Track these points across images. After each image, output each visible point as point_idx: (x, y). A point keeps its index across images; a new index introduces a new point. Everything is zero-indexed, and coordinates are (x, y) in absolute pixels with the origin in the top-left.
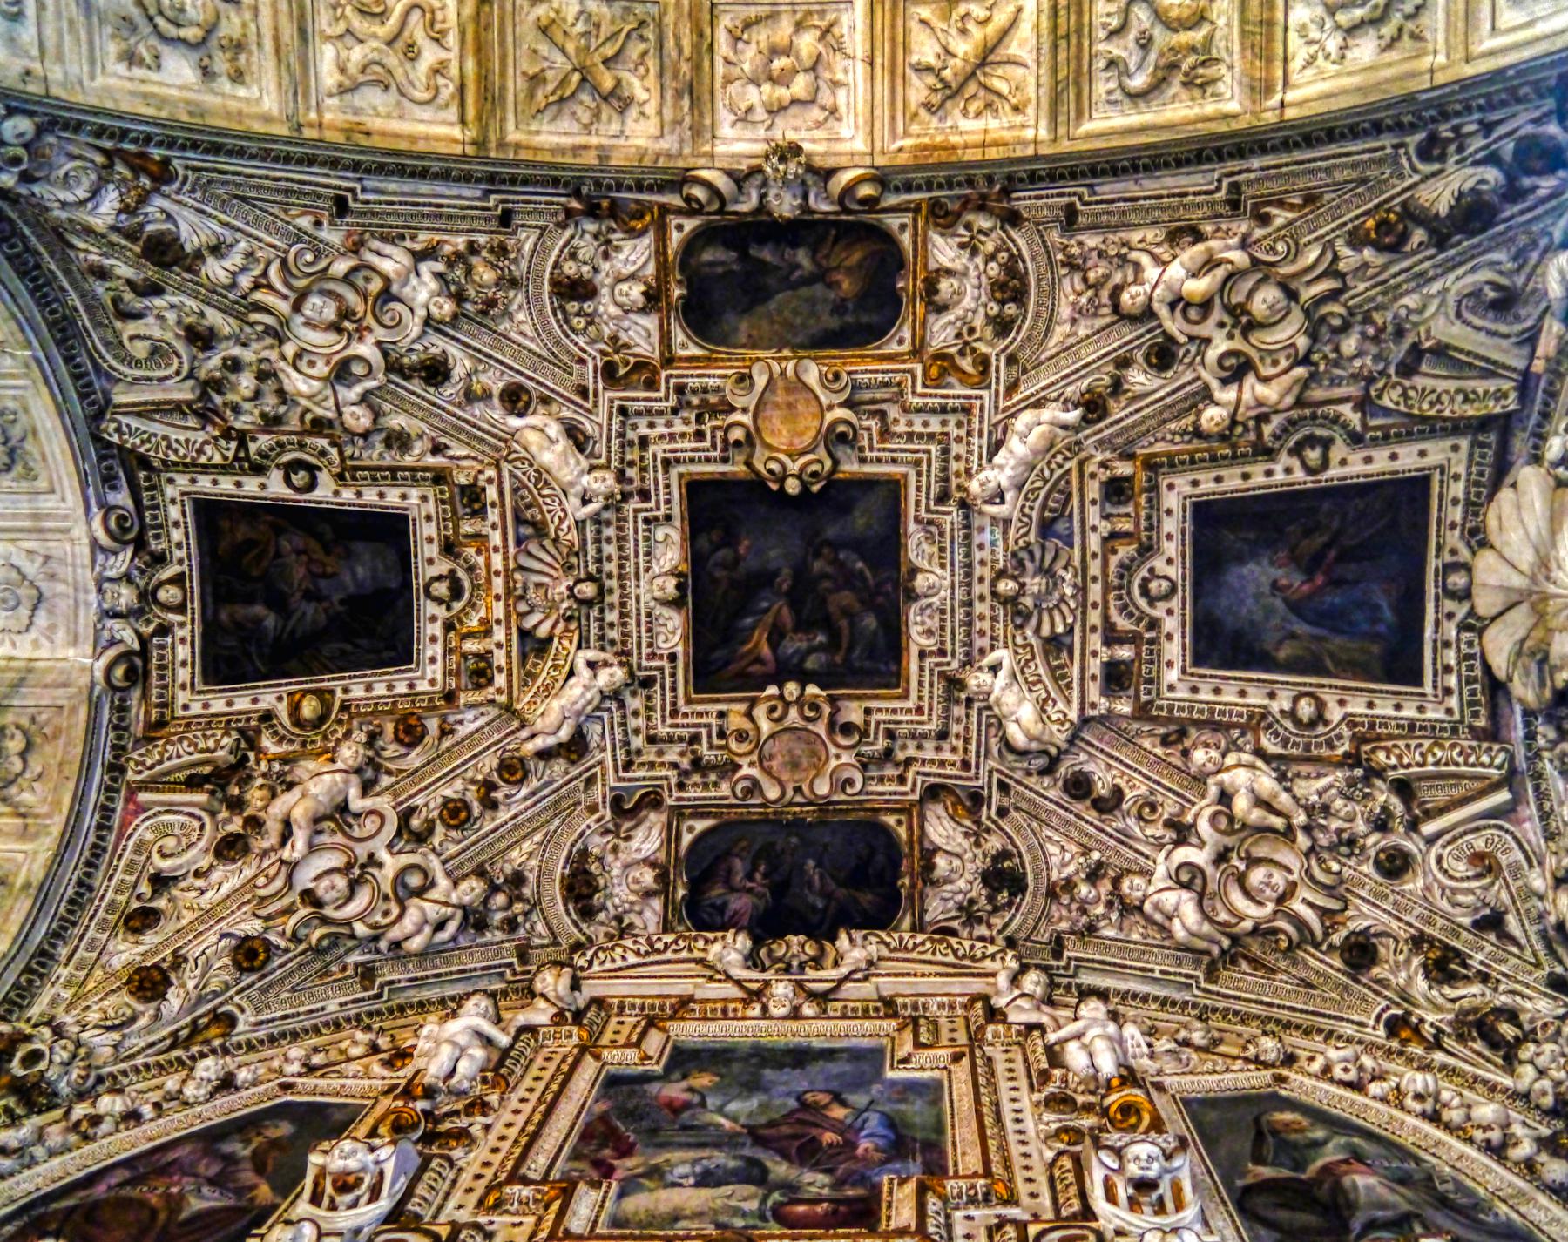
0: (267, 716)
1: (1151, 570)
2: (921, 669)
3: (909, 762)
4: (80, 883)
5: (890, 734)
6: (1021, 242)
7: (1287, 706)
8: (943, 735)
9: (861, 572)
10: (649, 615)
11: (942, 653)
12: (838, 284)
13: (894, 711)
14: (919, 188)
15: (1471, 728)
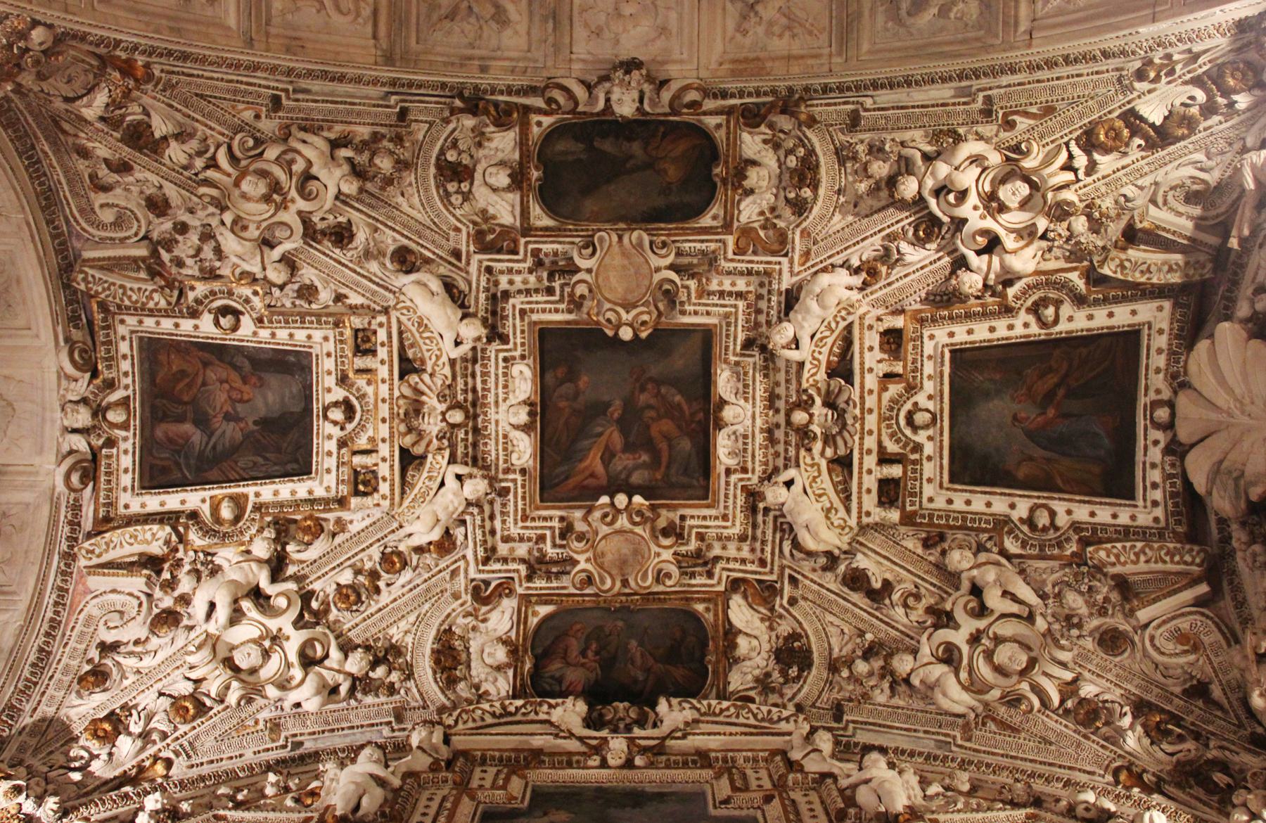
0: (194, 515)
1: (916, 404)
2: (727, 483)
3: (717, 559)
4: (41, 650)
5: (701, 537)
6: (815, 140)
7: (1025, 515)
8: (742, 538)
9: (679, 405)
10: (505, 436)
11: (745, 470)
12: (665, 171)
13: (704, 518)
14: (733, 96)
15: (1174, 532)
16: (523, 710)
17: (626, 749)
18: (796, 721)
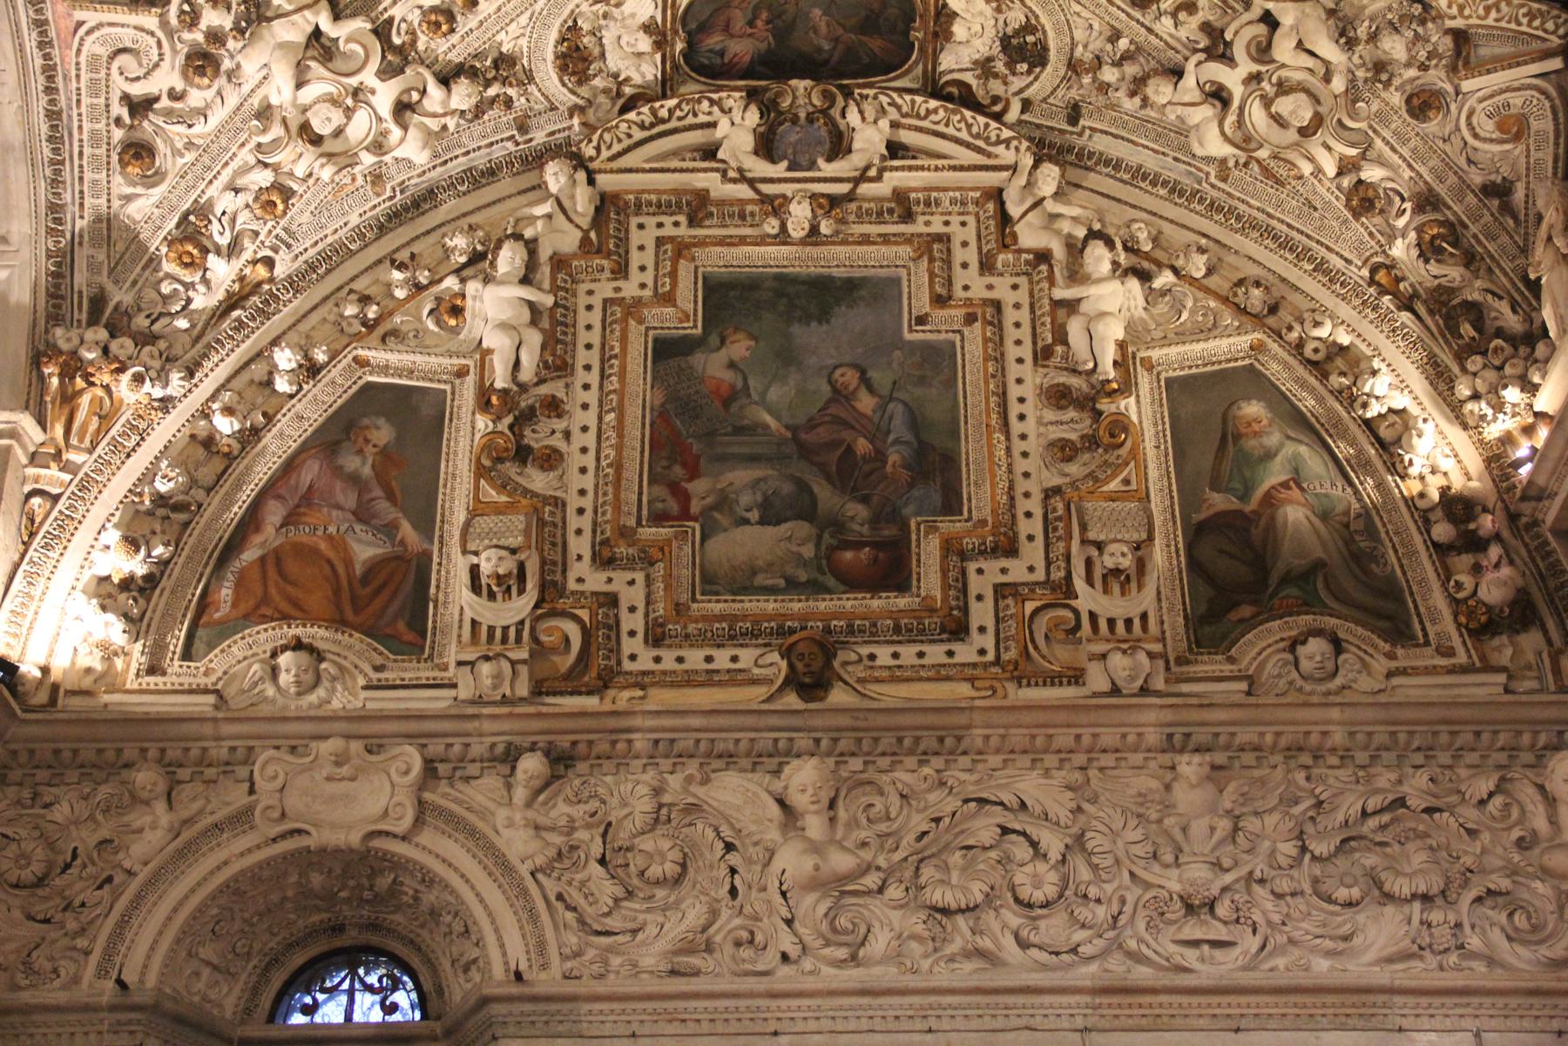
16: (678, 113)
17: (809, 214)
18: (1017, 149)
